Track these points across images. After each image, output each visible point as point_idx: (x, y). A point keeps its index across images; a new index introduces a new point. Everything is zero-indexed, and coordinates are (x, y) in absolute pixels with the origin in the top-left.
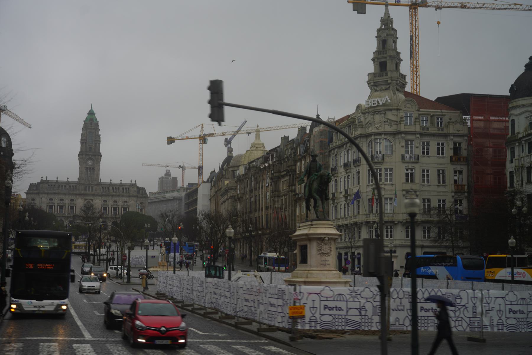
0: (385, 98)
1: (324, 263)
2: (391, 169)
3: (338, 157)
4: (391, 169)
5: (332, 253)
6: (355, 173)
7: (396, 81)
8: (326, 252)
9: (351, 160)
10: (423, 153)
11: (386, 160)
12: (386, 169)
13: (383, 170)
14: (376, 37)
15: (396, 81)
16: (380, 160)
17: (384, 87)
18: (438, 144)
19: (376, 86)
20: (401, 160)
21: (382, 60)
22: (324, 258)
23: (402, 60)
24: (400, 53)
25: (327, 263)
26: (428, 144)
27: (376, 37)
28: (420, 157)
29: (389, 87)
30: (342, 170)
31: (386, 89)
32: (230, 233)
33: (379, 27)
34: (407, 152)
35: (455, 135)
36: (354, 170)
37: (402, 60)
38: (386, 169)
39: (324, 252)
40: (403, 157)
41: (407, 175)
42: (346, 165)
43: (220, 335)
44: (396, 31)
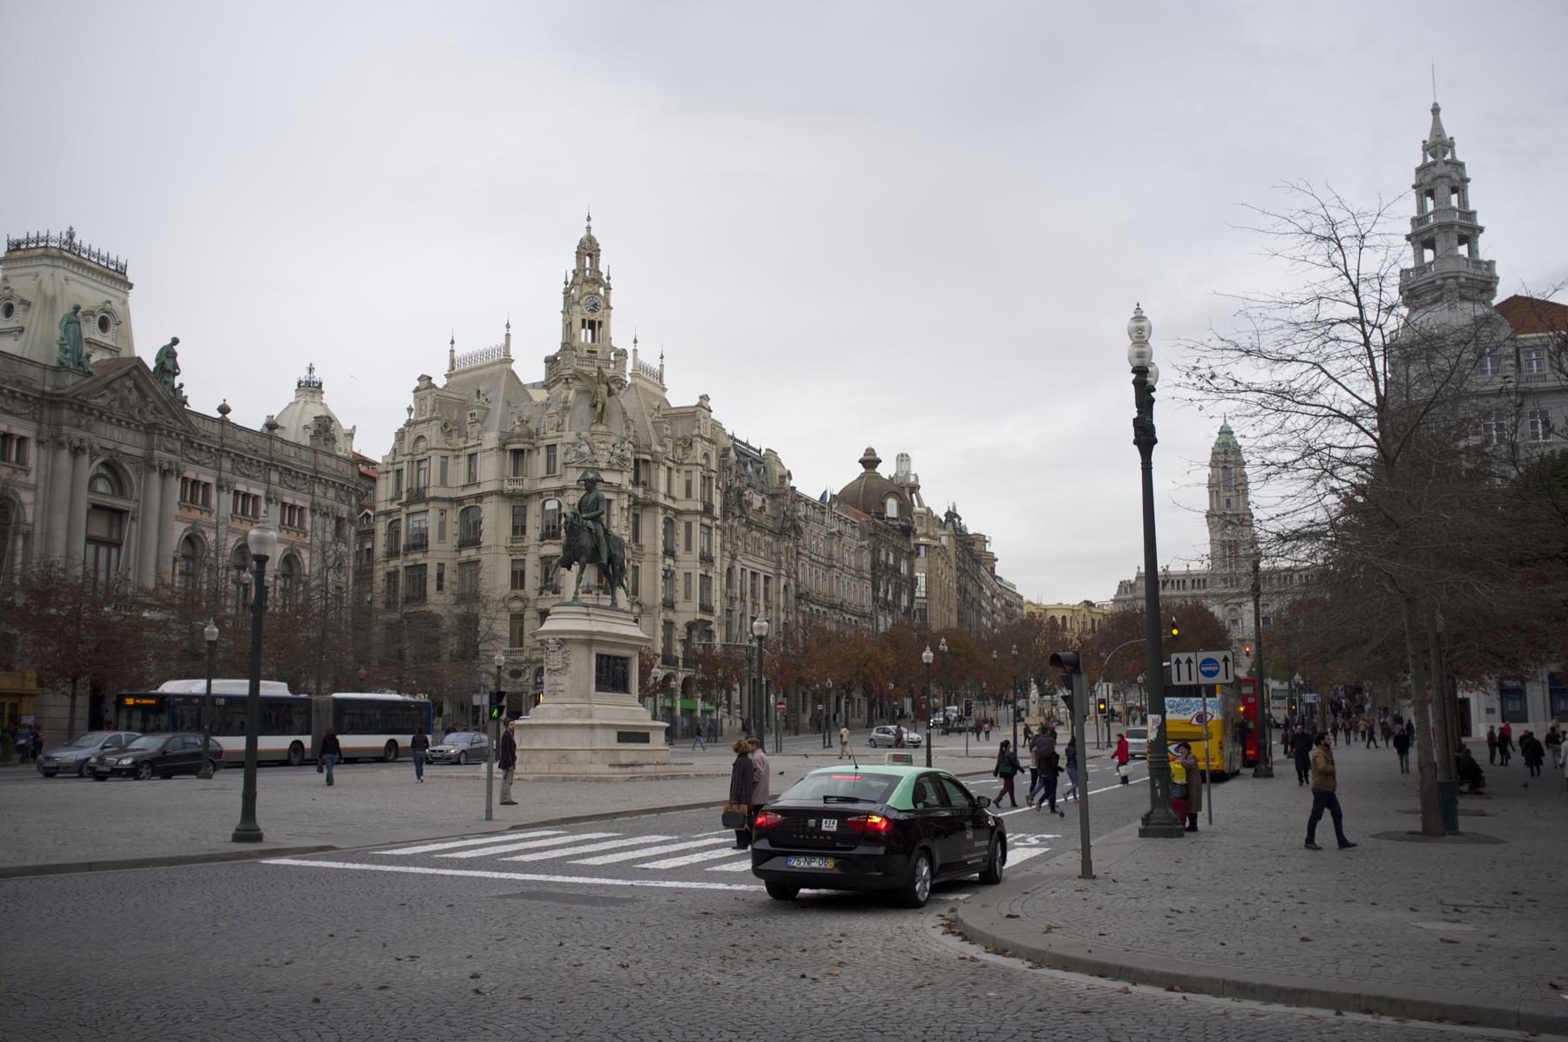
0: (1438, 318)
5: (572, 669)
7: (1456, 278)
14: (1414, 187)
15: (1456, 278)
17: (1428, 298)
19: (1417, 297)
21: (1426, 237)
23: (1481, 230)
24: (1474, 213)
27: (1414, 187)
29: (1441, 296)
31: (1436, 301)
32: (212, 634)
33: (1419, 163)
37: (1481, 230)
43: (594, 836)
44: (1462, 165)
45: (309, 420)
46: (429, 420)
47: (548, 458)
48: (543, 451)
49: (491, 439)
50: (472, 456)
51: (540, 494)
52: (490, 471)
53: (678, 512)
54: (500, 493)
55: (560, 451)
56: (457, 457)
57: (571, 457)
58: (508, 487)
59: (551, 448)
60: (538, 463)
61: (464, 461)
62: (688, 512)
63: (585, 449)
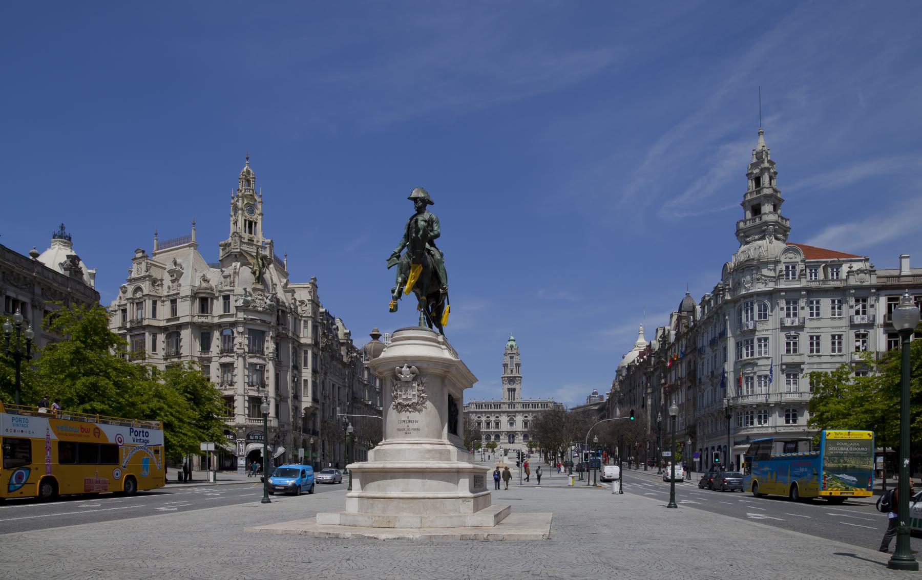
1: (404, 426)
2: (766, 339)
3: (705, 335)
4: (766, 339)
6: (722, 350)
8: (410, 402)
9: (717, 335)
10: (812, 314)
11: (758, 328)
12: (760, 340)
13: (756, 341)
16: (751, 327)
18: (833, 302)
20: (778, 326)
22: (404, 415)
25: (411, 426)
26: (818, 302)
28: (807, 321)
30: (708, 349)
34: (788, 315)
35: (856, 288)
36: (720, 346)
38: (760, 340)
39: (406, 403)
40: (782, 323)
41: (788, 344)
42: (713, 343)
45: (64, 259)
46: (144, 277)
47: (225, 303)
48: (221, 299)
49: (185, 291)
50: (174, 302)
51: (219, 326)
52: (186, 311)
53: (301, 345)
54: (192, 325)
55: (232, 299)
56: (163, 301)
57: (240, 303)
58: (196, 319)
59: (226, 298)
60: (217, 307)
61: (168, 304)
62: (306, 345)
63: (249, 298)
